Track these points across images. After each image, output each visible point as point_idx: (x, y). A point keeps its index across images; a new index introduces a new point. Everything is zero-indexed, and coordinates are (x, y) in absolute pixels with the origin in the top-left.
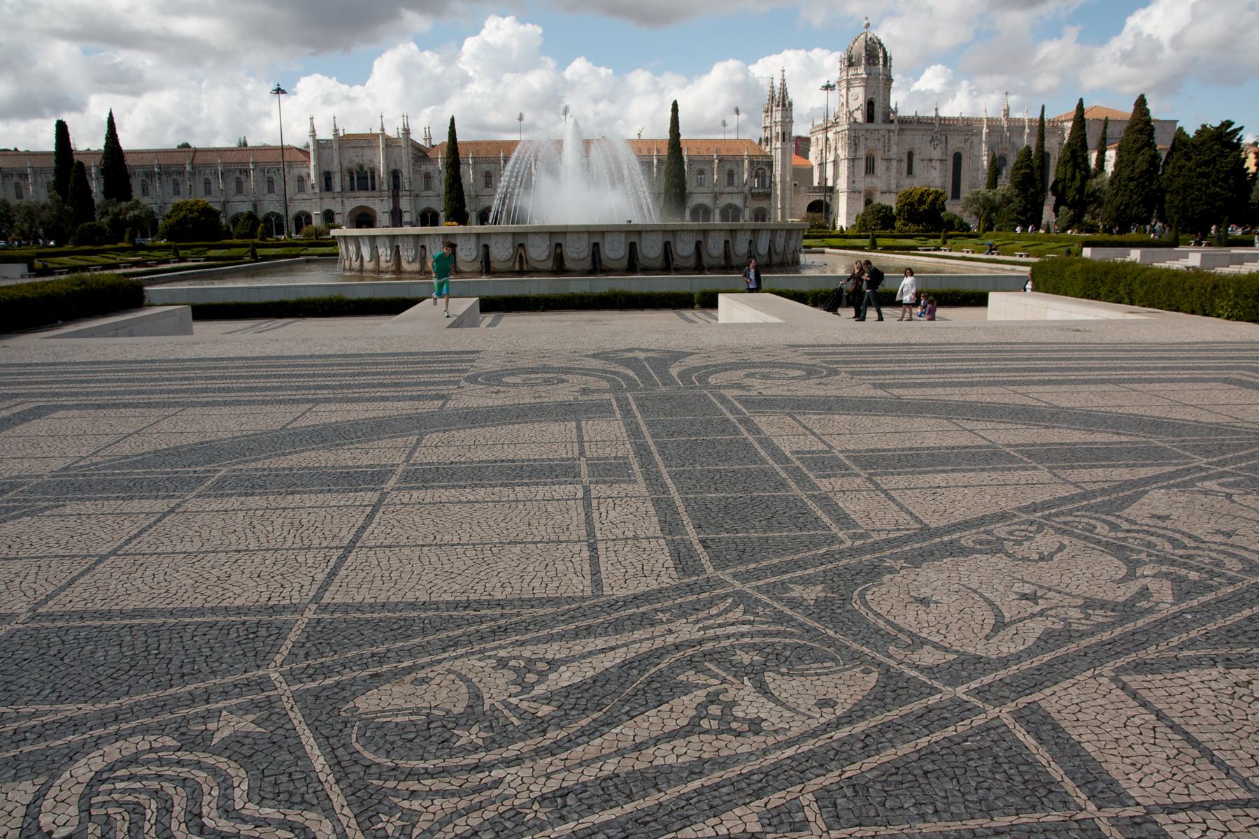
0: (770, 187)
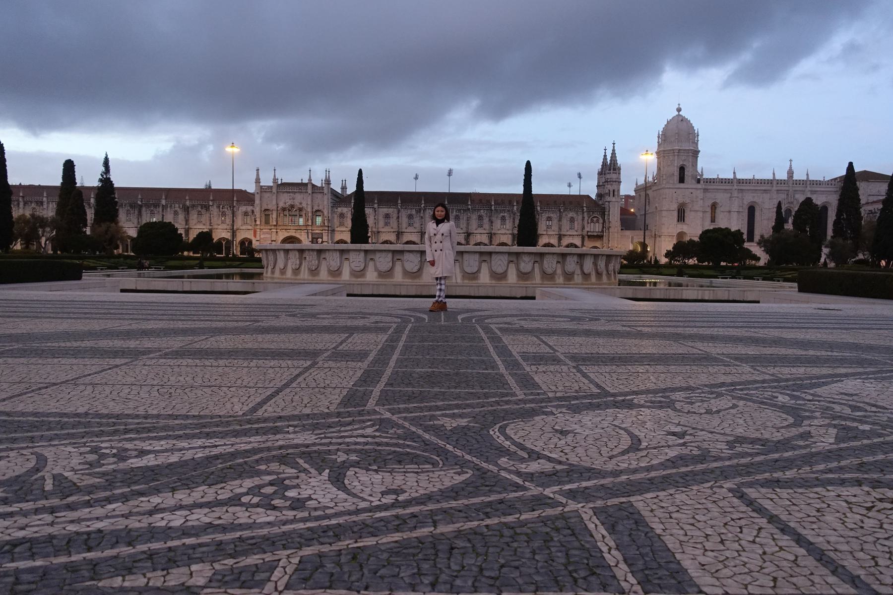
0: (602, 231)
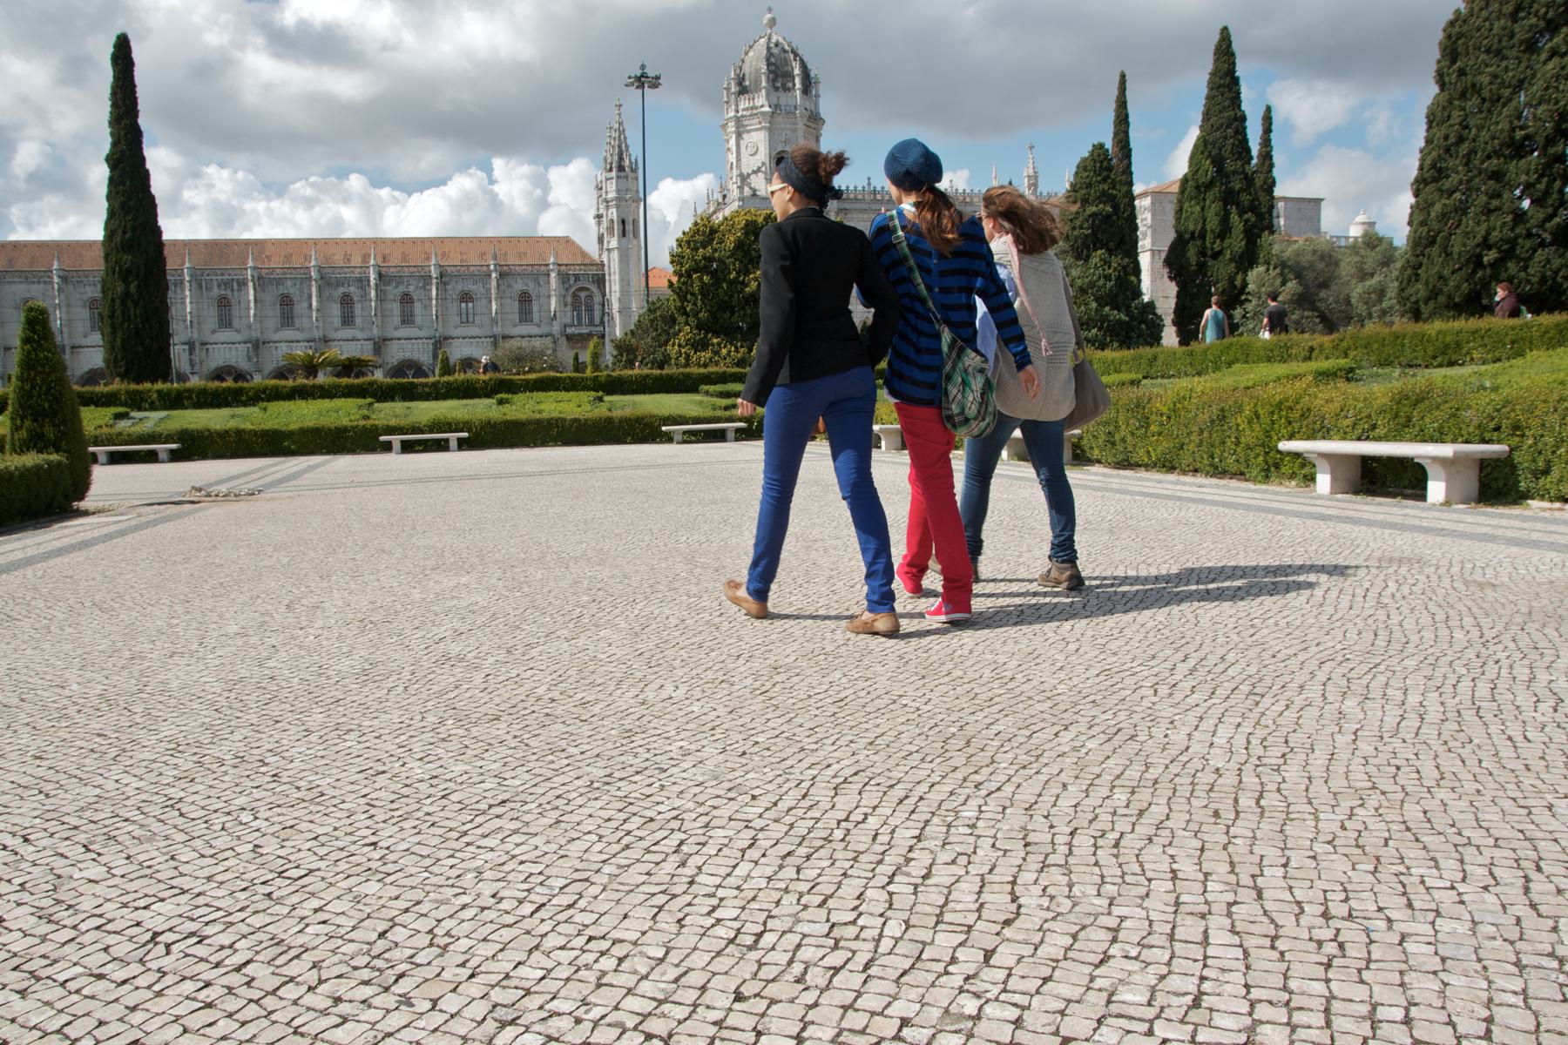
0: (602, 323)
